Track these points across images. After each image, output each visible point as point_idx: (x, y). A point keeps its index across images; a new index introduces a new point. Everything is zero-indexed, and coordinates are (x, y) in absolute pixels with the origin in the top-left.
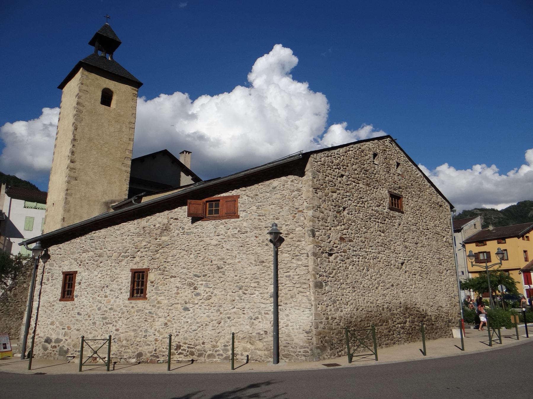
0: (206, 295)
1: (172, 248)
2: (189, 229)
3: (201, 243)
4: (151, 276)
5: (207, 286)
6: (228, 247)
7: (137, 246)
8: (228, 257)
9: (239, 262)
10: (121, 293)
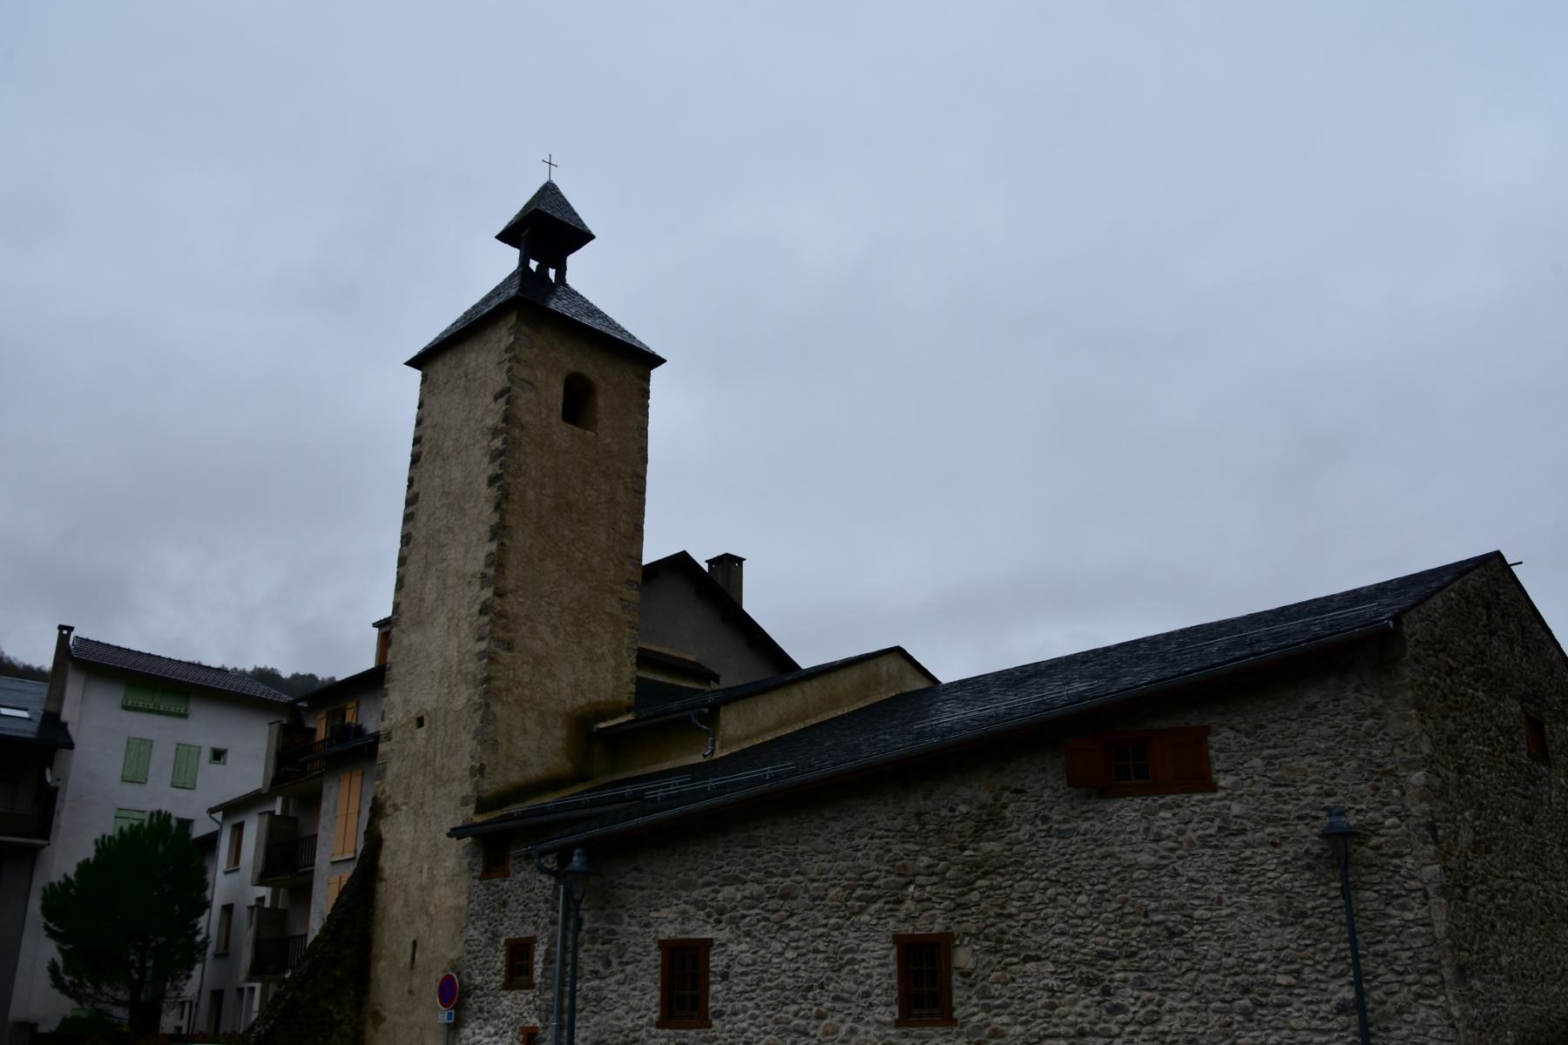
0: (1143, 1012)
1: (1019, 876)
2: (1065, 821)
3: (1106, 862)
4: (963, 957)
5: (1141, 984)
6: (1192, 874)
7: (904, 867)
8: (1196, 902)
9: (1232, 915)
10: (871, 1005)
